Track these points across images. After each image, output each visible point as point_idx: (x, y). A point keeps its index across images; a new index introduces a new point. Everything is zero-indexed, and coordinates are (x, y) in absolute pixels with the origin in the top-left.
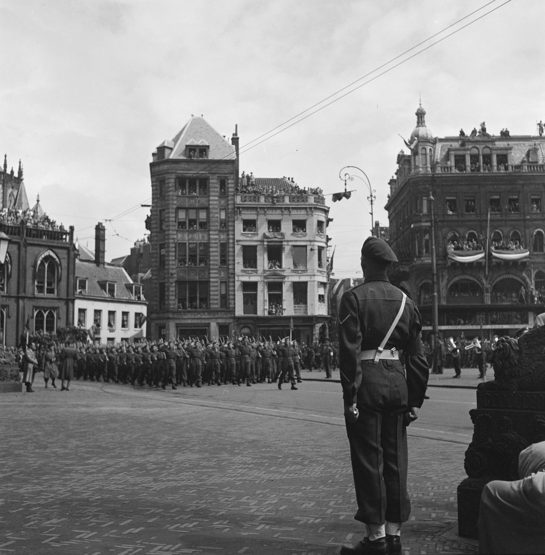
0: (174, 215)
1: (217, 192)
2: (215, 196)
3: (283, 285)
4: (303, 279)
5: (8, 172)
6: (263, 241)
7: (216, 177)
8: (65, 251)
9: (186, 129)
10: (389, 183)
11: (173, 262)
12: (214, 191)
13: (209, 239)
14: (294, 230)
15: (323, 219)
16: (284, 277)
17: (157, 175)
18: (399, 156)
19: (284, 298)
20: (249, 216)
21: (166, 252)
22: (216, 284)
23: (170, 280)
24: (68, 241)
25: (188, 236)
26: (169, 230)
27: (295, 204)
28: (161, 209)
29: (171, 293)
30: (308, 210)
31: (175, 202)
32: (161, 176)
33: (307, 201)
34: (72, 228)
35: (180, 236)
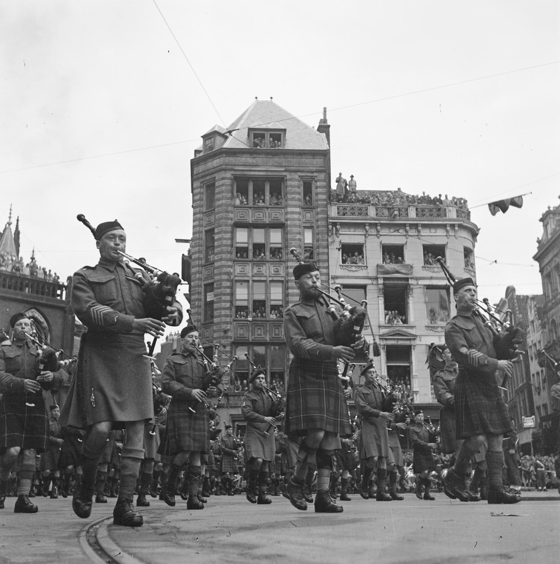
1: (299, 200)
2: (295, 206)
3: (413, 352)
6: (377, 278)
8: (59, 314)
9: (247, 114)
10: (541, 220)
11: (228, 312)
12: (293, 199)
14: (426, 262)
16: (414, 337)
17: (203, 177)
19: (414, 374)
20: (352, 237)
21: (215, 296)
23: (223, 341)
24: (64, 298)
28: (207, 228)
30: (448, 228)
31: (231, 215)
32: (208, 178)
33: (446, 215)
35: (238, 269)
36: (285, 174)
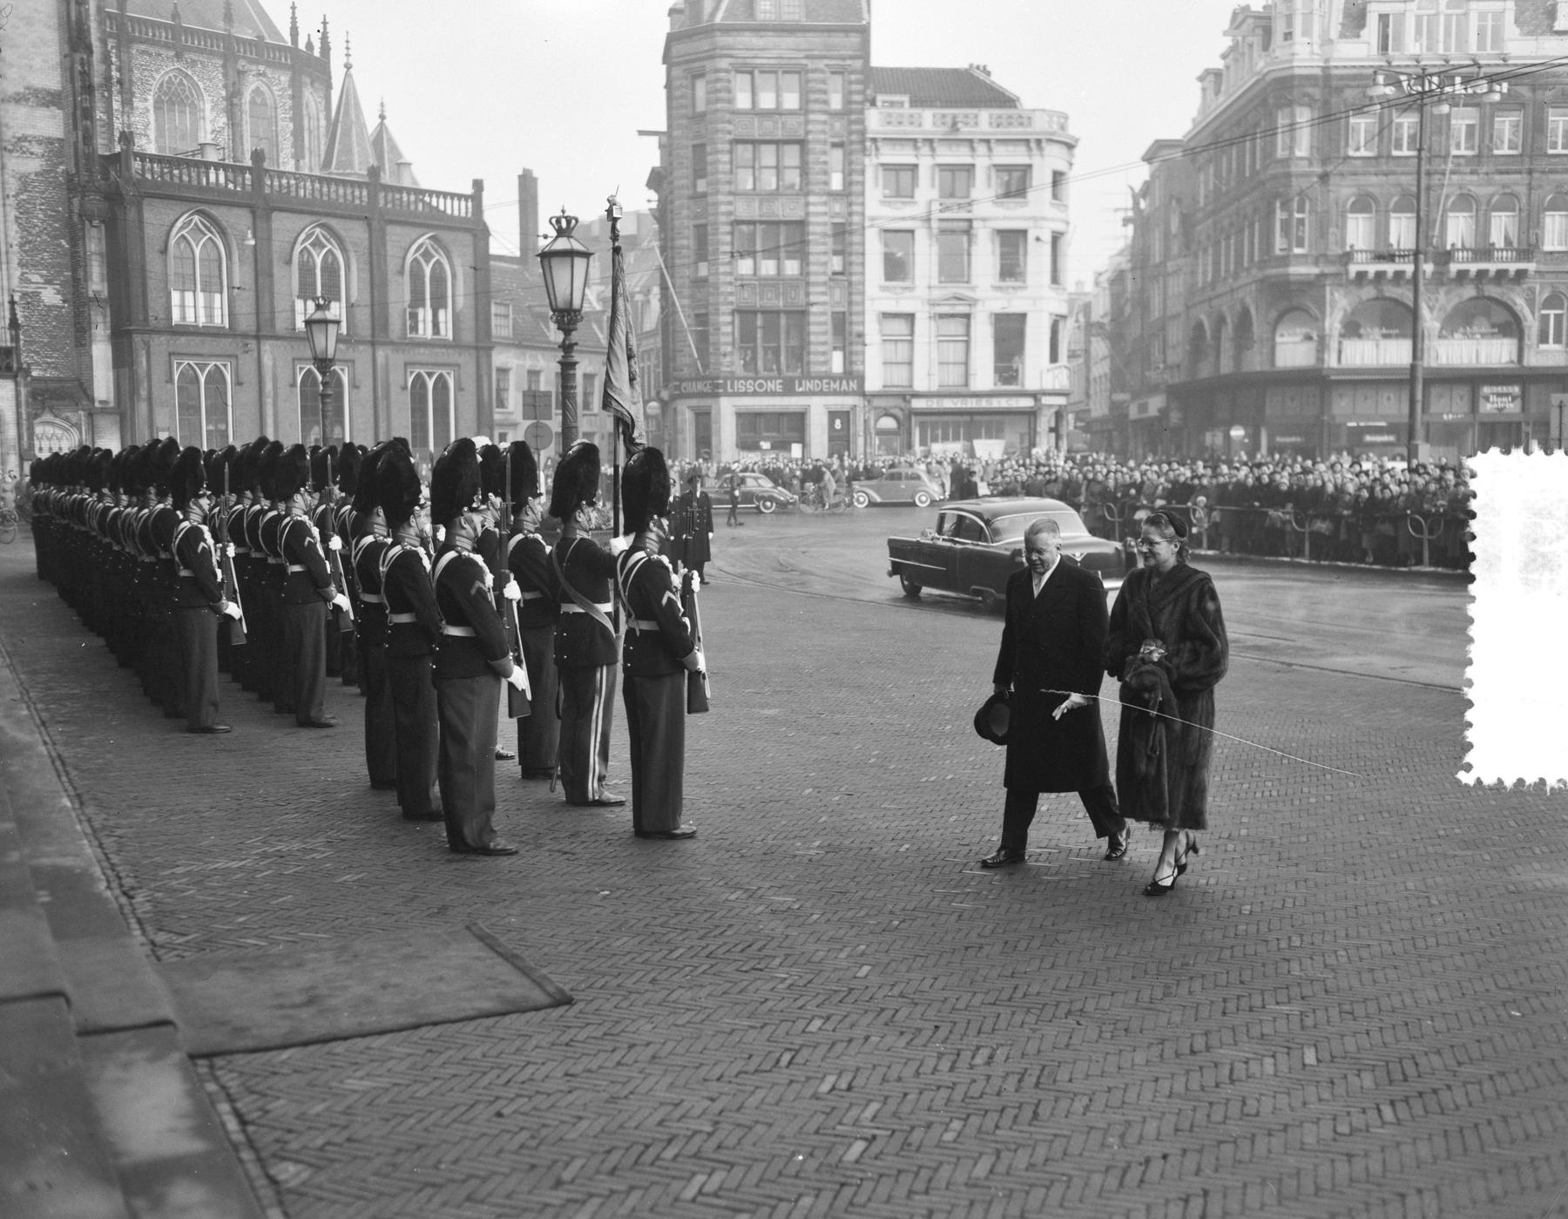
0: (726, 158)
4: (1016, 307)
5: (302, 46)
7: (821, 64)
10: (1201, 79)
13: (807, 214)
15: (1061, 166)
16: (973, 302)
18: (1235, 15)
22: (822, 319)
25: (761, 204)
26: (717, 193)
27: (1002, 133)
29: (723, 339)
30: (1033, 145)
32: (696, 65)
34: (478, 185)
36: (804, 62)
